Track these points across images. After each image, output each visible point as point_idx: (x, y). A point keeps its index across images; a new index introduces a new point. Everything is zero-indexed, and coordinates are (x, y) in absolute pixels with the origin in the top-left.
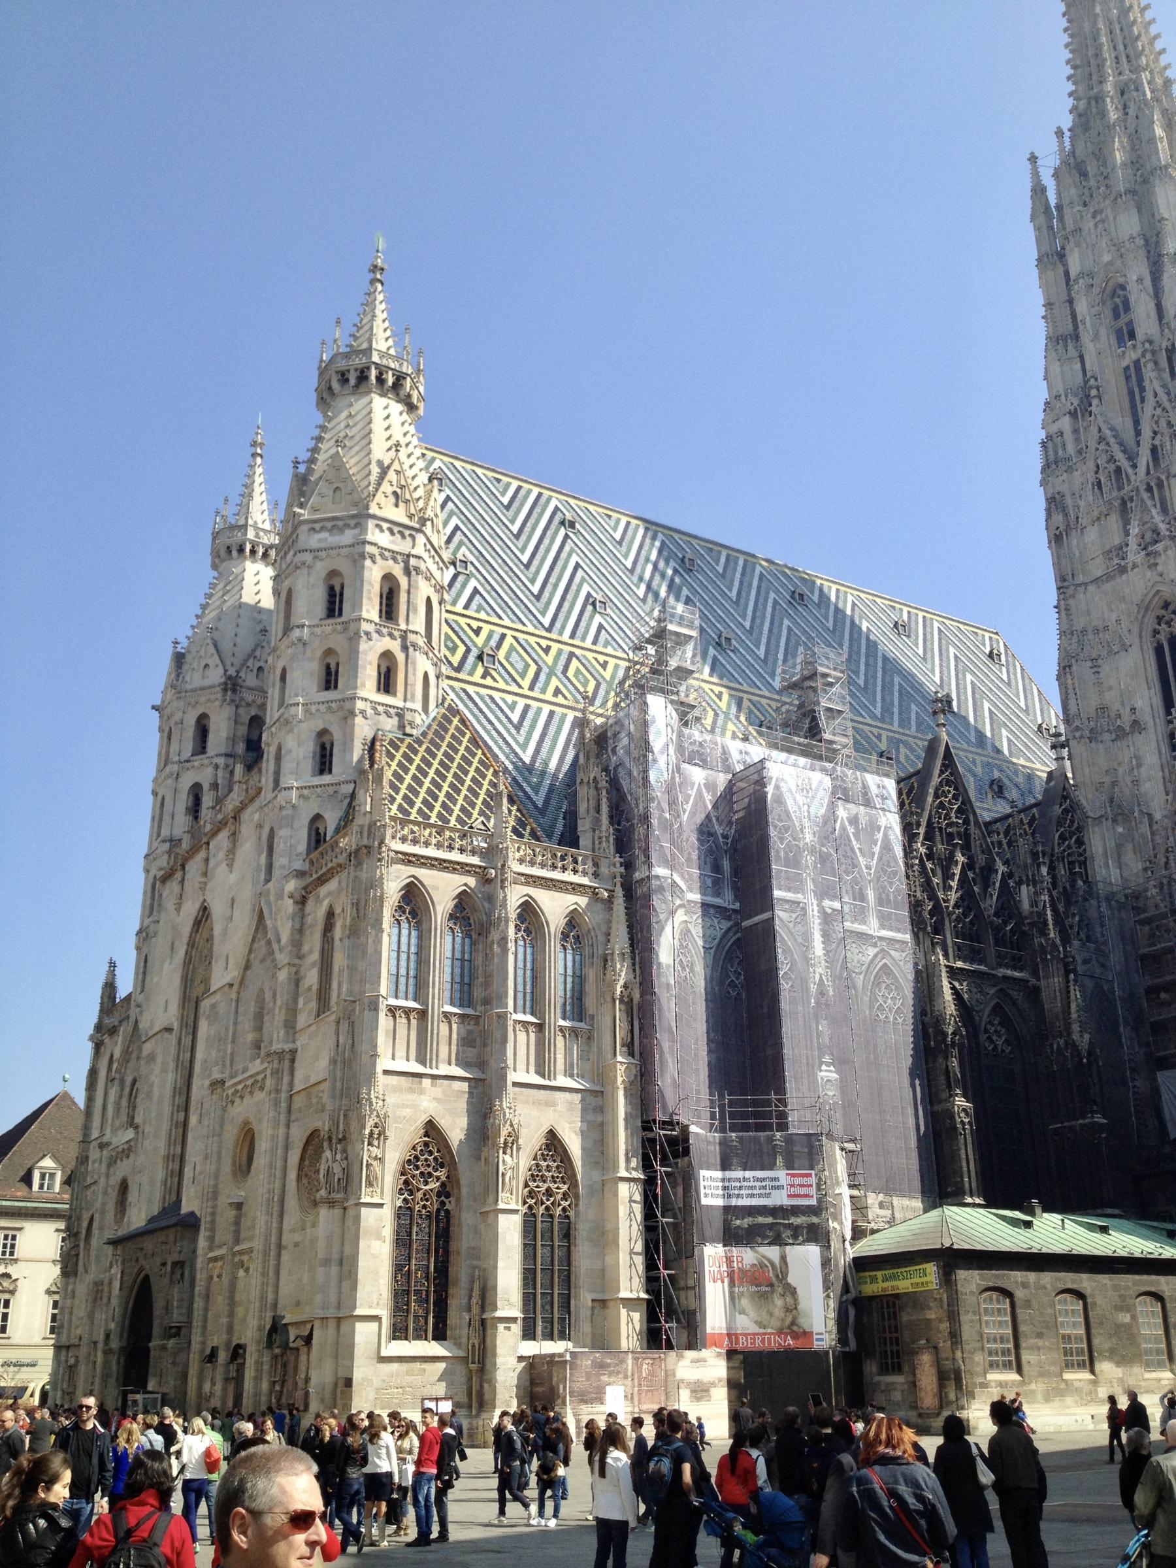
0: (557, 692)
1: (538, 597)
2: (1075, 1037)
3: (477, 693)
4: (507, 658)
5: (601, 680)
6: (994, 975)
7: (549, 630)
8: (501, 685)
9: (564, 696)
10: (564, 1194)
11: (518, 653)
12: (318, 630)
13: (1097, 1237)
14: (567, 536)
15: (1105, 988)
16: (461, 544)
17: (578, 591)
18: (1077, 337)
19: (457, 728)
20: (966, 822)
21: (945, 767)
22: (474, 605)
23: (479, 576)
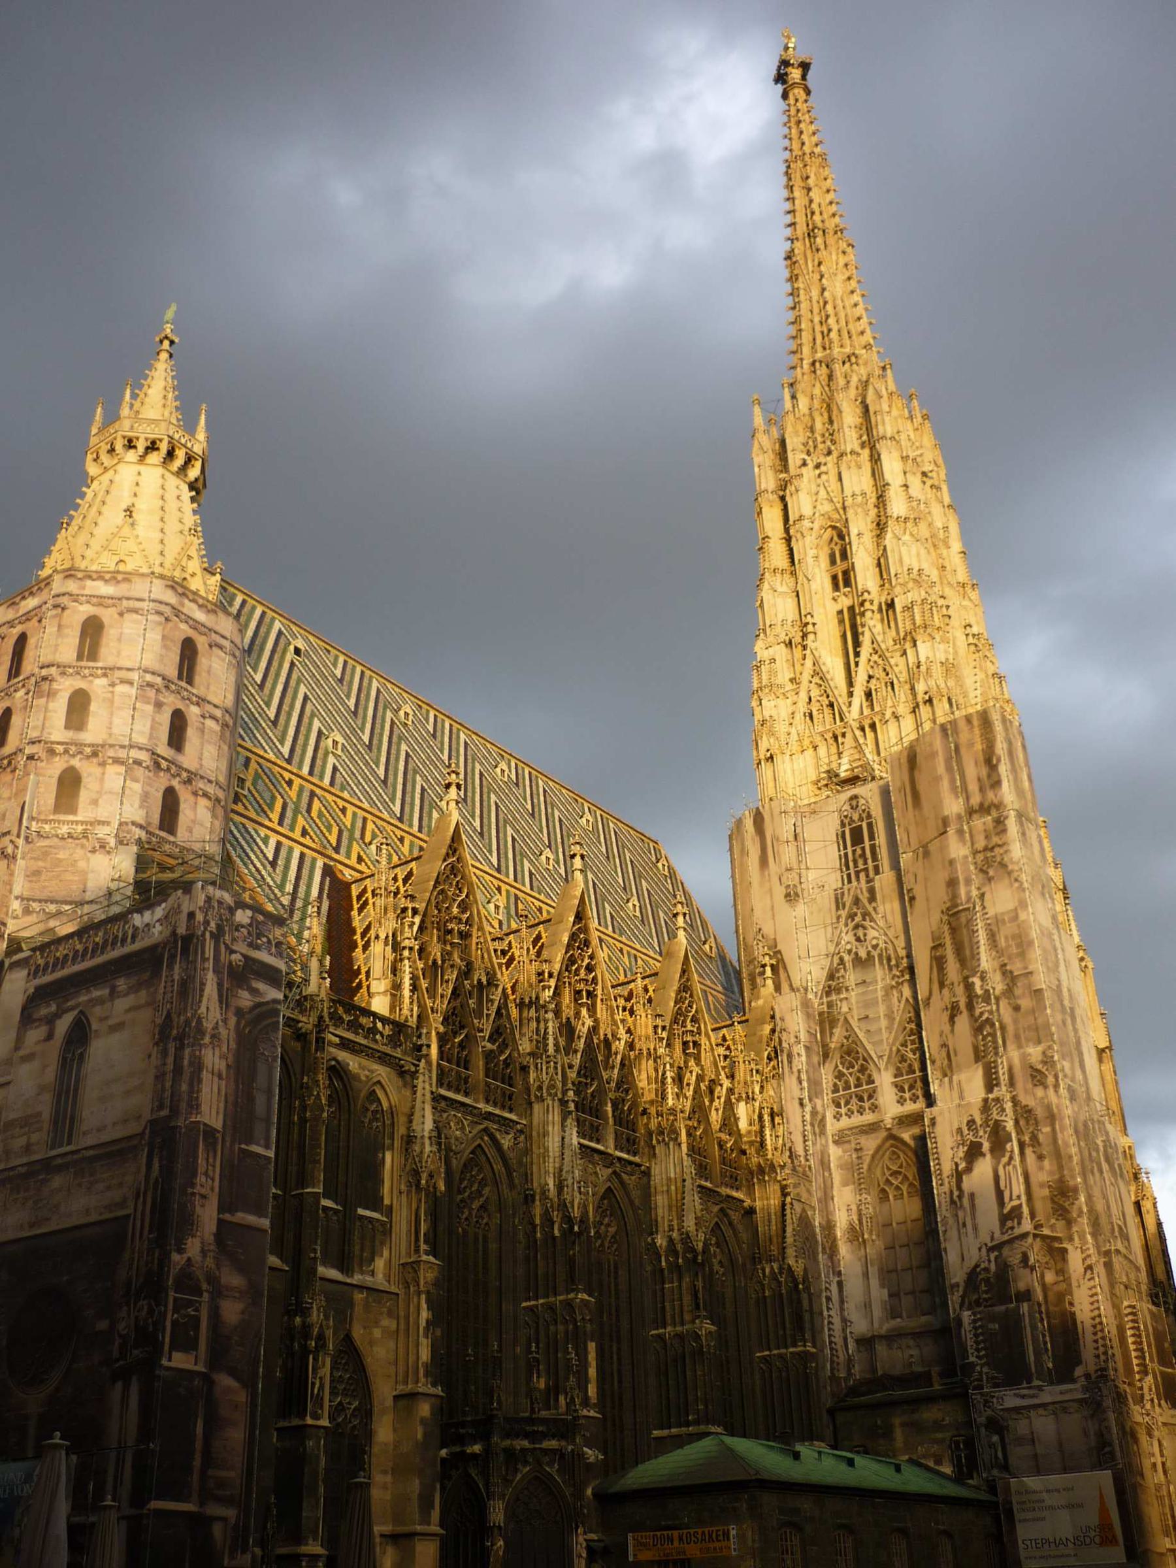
0: (304, 833)
2: (791, 1261)
4: (254, 784)
7: (289, 761)
8: (253, 815)
10: (355, 1409)
11: (264, 781)
13: (843, 1467)
14: (292, 664)
15: (809, 1213)
17: (310, 724)
18: (793, 573)
21: (684, 972)
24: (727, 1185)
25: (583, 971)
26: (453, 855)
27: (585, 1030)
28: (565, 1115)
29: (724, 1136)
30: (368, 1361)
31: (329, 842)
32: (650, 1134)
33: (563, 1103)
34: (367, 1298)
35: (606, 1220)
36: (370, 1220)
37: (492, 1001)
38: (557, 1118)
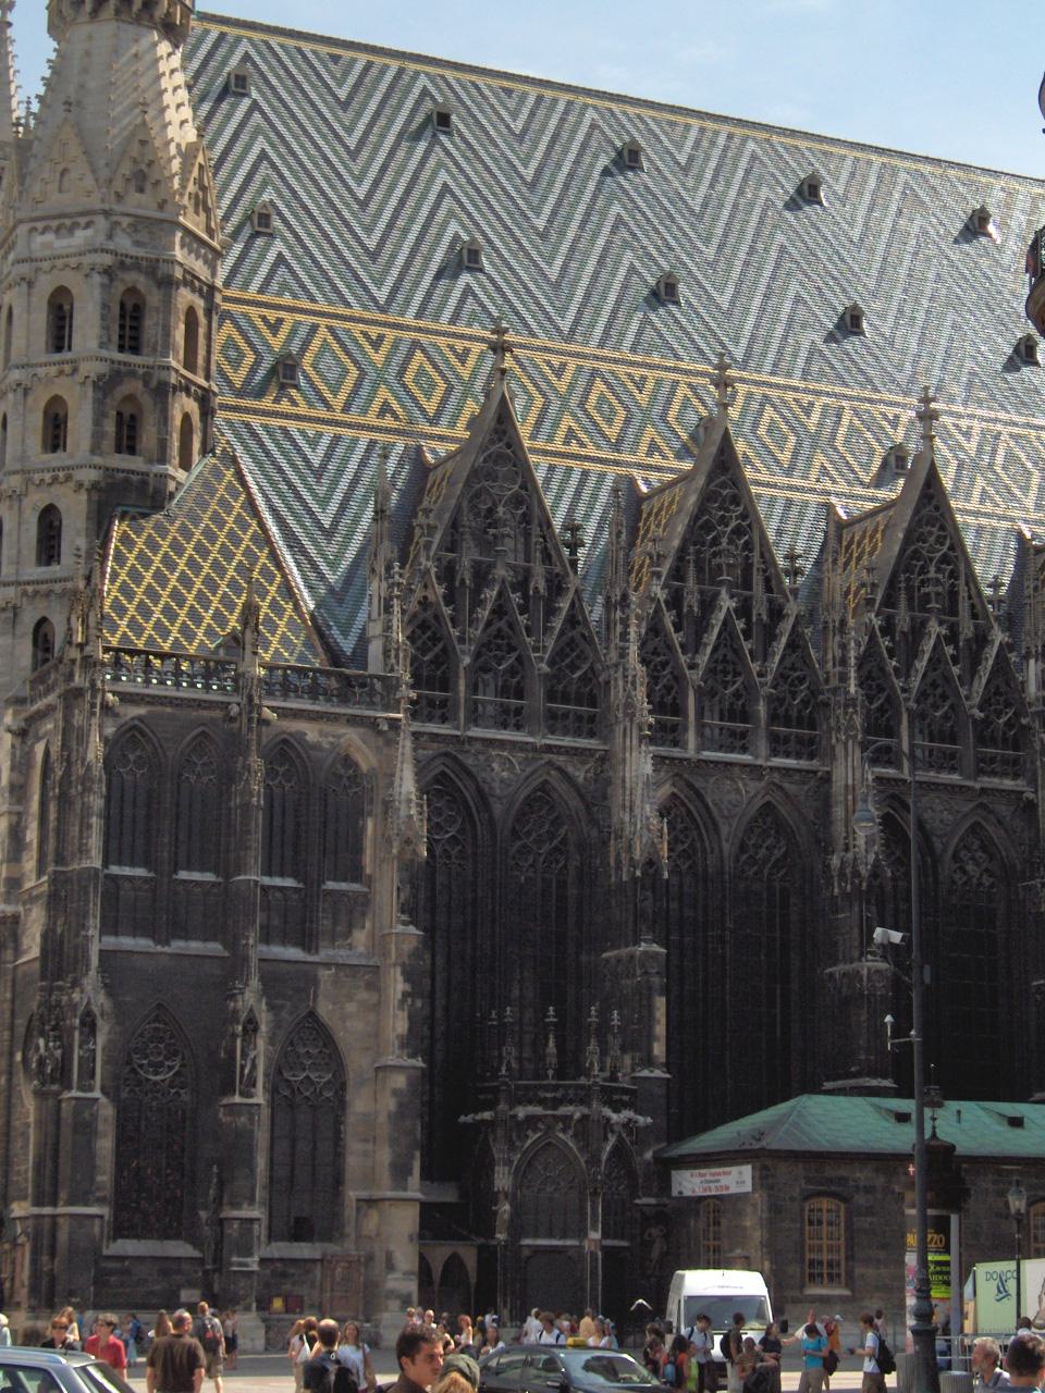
0: (385, 409)
1: (374, 256)
3: (265, 427)
4: (314, 366)
5: (454, 381)
6: (969, 788)
8: (303, 409)
9: (394, 414)
10: (329, 1082)
12: (41, 371)
13: (1004, 1128)
16: (265, 183)
17: (440, 236)
19: (230, 488)
20: (953, 575)
22: (274, 286)
23: (288, 235)
24: (994, 773)
25: (724, 540)
26: (500, 440)
27: (722, 616)
28: (641, 739)
29: (979, 715)
30: (340, 1035)
31: (423, 411)
32: (830, 729)
33: (641, 729)
34: (336, 974)
35: (769, 842)
36: (343, 893)
37: (560, 609)
38: (635, 742)
